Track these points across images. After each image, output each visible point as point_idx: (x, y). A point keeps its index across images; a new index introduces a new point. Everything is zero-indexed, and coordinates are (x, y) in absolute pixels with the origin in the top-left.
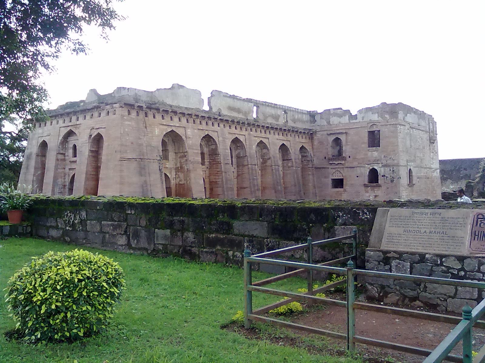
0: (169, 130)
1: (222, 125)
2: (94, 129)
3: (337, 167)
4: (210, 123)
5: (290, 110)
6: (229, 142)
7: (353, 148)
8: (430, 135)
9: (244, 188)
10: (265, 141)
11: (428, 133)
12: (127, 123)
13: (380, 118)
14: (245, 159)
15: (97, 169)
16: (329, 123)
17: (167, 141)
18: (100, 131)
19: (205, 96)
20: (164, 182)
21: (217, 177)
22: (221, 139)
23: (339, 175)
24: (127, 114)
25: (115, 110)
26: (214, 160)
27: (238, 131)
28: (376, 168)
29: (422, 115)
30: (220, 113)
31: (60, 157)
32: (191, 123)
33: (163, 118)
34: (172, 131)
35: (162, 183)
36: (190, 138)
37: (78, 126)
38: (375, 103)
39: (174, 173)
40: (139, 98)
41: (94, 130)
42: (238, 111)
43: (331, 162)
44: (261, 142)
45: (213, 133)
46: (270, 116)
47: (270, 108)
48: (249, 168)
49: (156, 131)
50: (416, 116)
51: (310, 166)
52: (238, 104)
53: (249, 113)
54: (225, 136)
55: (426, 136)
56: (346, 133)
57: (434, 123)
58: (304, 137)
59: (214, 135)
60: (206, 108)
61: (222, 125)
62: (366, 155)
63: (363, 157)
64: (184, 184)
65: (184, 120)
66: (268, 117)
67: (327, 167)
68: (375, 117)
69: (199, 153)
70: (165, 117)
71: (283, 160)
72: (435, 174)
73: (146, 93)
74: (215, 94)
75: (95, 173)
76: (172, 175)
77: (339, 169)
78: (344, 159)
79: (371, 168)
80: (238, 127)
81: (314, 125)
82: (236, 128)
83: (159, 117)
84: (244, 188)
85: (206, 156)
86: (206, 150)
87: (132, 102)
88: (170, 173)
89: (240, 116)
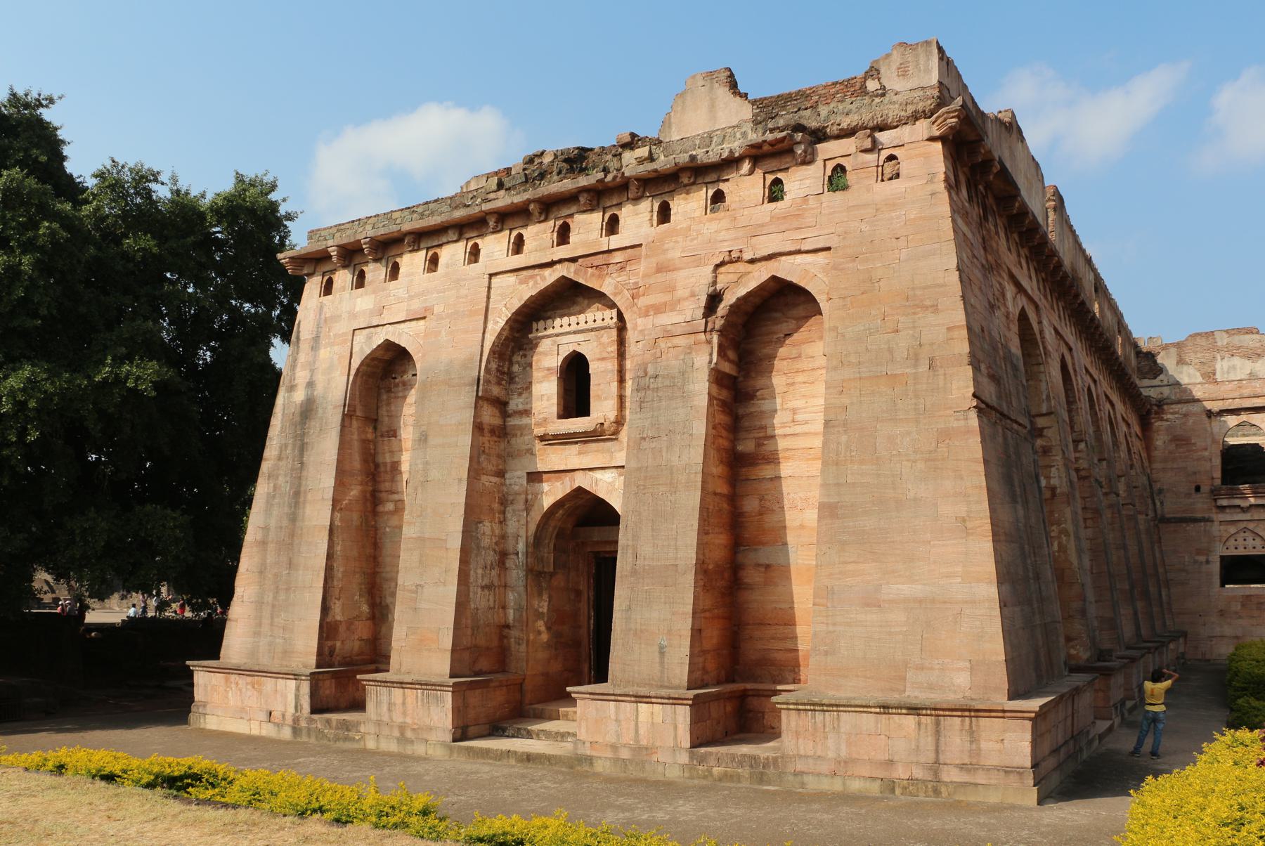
2: (739, 260)
3: (1247, 516)
23: (1250, 542)
25: (891, 158)
37: (618, 257)
41: (741, 267)
43: (1224, 503)
67: (1206, 516)
77: (1251, 526)
81: (1156, 382)
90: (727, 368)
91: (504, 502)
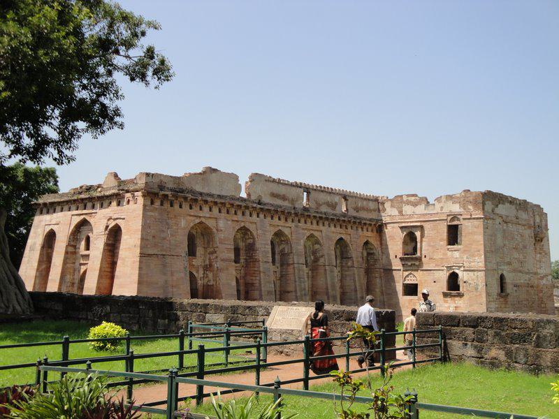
0: (197, 221)
1: (262, 216)
4: (247, 212)
5: (352, 197)
6: (270, 236)
7: (430, 246)
8: (535, 230)
9: (289, 292)
10: (316, 234)
11: (533, 228)
12: (149, 213)
13: (462, 210)
14: (291, 257)
15: (113, 265)
16: (401, 212)
17: (194, 233)
18: (118, 222)
19: (243, 180)
21: (254, 278)
22: (259, 232)
23: (413, 278)
24: (150, 203)
26: (251, 257)
27: (282, 222)
28: (457, 271)
29: (523, 205)
30: (260, 201)
31: (71, 249)
33: (191, 208)
34: (201, 223)
36: (221, 230)
38: (457, 190)
39: (201, 272)
41: (112, 220)
42: (284, 198)
44: (312, 236)
46: (324, 204)
47: (325, 194)
48: (294, 268)
50: (513, 207)
51: (378, 266)
52: (282, 190)
53: (297, 201)
55: (528, 233)
56: (422, 227)
57: (543, 216)
58: (370, 229)
59: (252, 228)
60: (243, 195)
61: (262, 216)
62: (444, 254)
63: (441, 257)
64: (213, 285)
66: (321, 205)
68: (456, 208)
70: (194, 207)
71: (342, 258)
72: (544, 281)
73: (172, 179)
74: (255, 178)
75: (109, 270)
76: (199, 275)
78: (420, 259)
79: (451, 271)
80: (282, 217)
82: (279, 219)
83: (186, 206)
84: (289, 292)
85: (242, 252)
86: (242, 245)
87: (156, 190)
88: (197, 272)
89: (286, 204)
90: (110, 242)
91: (75, 270)
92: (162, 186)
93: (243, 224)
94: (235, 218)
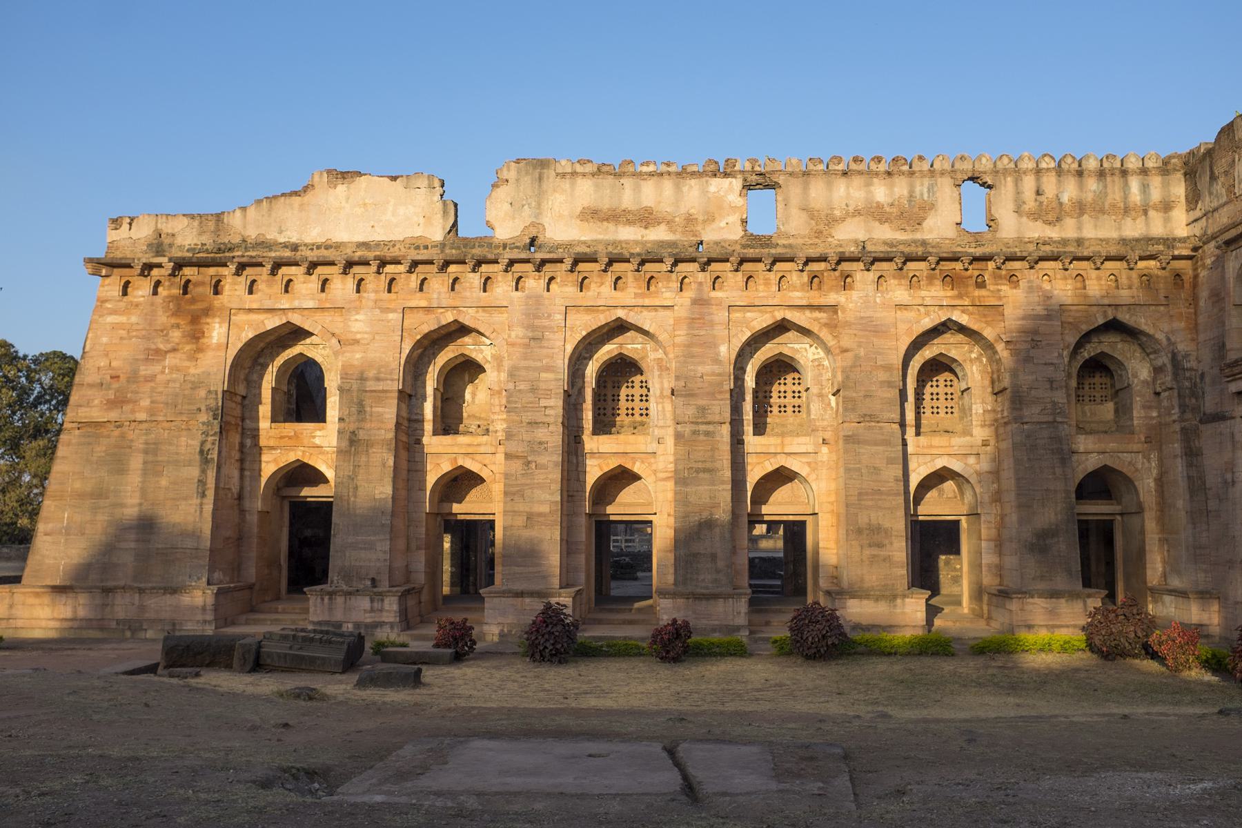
0: (272, 322)
12: (110, 319)
20: (210, 494)
32: (376, 292)
35: (203, 495)
36: (357, 342)
40: (167, 241)
42: (646, 218)
45: (481, 315)
49: (215, 334)
53: (710, 219)
54: (546, 323)
65: (342, 287)
69: (391, 391)
73: (196, 223)
92: (160, 245)
93: (449, 317)
94: (419, 301)
